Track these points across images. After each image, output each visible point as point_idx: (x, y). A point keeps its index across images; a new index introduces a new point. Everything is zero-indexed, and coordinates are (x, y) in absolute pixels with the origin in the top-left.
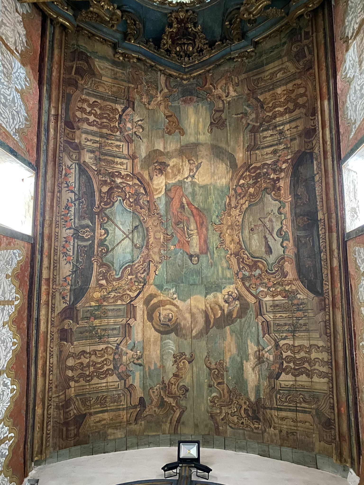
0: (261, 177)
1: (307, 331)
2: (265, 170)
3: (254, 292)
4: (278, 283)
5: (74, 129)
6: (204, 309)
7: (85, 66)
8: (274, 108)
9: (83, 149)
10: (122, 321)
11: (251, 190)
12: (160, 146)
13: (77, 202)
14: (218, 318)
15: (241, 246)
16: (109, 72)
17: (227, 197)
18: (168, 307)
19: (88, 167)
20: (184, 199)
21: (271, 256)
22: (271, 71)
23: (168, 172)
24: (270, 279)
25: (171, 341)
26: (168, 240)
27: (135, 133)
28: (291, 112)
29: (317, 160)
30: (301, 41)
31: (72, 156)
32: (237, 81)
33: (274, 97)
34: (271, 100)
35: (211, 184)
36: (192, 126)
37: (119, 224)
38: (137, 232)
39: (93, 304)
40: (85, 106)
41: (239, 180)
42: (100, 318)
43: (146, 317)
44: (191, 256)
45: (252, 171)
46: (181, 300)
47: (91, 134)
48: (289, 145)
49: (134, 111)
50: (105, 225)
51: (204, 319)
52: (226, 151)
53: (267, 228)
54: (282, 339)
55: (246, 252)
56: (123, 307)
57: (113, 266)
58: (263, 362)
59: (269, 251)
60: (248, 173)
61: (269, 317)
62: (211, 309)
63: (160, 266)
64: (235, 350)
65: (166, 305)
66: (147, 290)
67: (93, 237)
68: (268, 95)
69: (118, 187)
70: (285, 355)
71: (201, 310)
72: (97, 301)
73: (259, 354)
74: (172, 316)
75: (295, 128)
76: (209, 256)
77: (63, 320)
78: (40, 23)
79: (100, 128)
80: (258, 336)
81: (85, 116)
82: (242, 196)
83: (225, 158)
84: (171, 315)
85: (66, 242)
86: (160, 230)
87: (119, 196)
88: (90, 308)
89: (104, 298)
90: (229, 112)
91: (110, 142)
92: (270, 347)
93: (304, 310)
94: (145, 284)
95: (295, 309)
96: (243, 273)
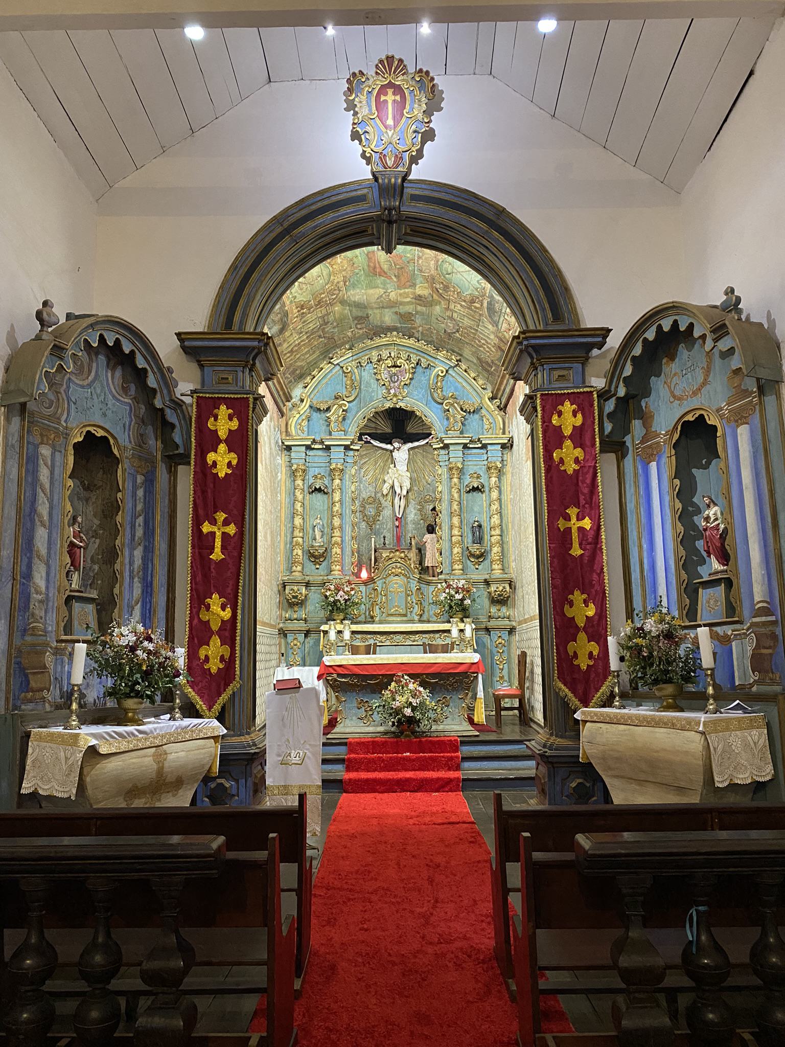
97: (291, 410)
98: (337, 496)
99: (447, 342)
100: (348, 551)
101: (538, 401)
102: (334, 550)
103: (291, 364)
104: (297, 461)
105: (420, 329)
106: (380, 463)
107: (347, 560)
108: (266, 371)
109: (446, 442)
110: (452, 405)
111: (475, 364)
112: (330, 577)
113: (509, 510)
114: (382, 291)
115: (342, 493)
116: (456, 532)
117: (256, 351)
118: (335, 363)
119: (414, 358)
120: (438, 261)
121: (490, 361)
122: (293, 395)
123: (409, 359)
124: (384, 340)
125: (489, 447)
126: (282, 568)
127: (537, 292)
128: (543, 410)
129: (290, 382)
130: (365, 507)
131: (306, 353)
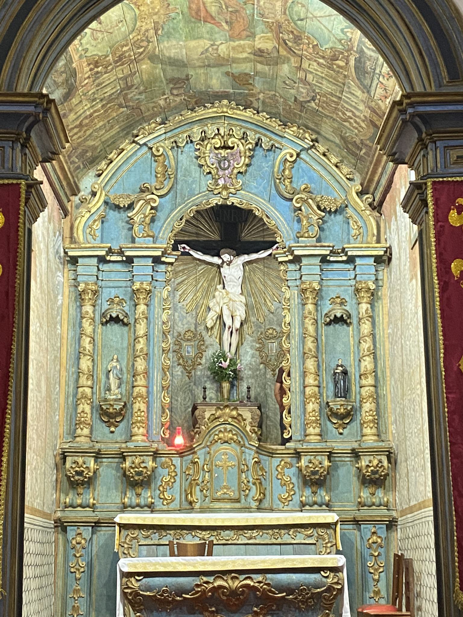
7: (350, 146)
13: (377, 71)
16: (323, 129)
19: (358, 87)
27: (295, 83)
28: (86, 118)
32: (155, 109)
37: (325, 31)
38: (299, 16)
40: (355, 125)
41: (144, 51)
49: (296, 98)
68: (115, 114)
78: (383, 208)
81: (358, 120)
91: (330, 90)
97: (77, 207)
98: (141, 329)
99: (296, 114)
100: (156, 407)
101: (429, 191)
102: (136, 406)
103: (79, 144)
104: (84, 278)
105: (261, 96)
106: (203, 283)
107: (155, 419)
108: (43, 147)
109: (296, 253)
110: (305, 201)
111: (337, 145)
112: (131, 445)
113: (385, 348)
114: (208, 43)
115: (148, 324)
116: (310, 380)
117: (31, 119)
118: (141, 143)
119: (252, 137)
121: (358, 142)
122: (82, 186)
123: (244, 137)
124: (210, 111)
125: (358, 261)
126: (61, 431)
127: (426, 40)
128: (436, 204)
129: (78, 168)
130: (181, 346)
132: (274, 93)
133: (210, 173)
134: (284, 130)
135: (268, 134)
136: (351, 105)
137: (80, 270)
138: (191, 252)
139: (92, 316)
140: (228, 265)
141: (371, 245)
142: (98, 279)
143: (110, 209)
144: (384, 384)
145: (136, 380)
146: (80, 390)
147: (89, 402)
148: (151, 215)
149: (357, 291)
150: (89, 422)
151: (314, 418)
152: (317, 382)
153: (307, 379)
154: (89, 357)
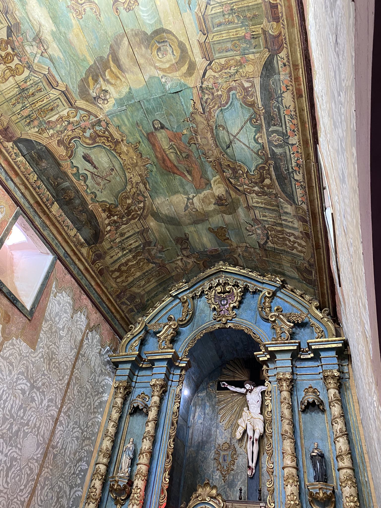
0: (125, 214)
1: (8, 99)
2: (124, 220)
3: (82, 112)
4: (62, 132)
5: (305, 233)
6: (126, 74)
7: (305, 274)
8: (137, 262)
9: (294, 216)
10: (213, 37)
11: (129, 201)
12: (228, 218)
14: (107, 69)
15: (116, 152)
16: (285, 269)
17: (149, 189)
18: (167, 65)
19: (287, 201)
20: (190, 178)
21: (83, 154)
22: (151, 283)
23: (213, 199)
24: (73, 132)
25: (148, 22)
26: (192, 138)
27: (252, 226)
29: (82, 245)
30: (135, 306)
31: (302, 212)
33: (141, 269)
34: (142, 266)
35: (169, 197)
36: (203, 235)
38: (226, 142)
39: (251, 56)
40: (300, 248)
41: (144, 206)
42: (239, 39)
43: (188, 47)
44: (163, 127)
45: (136, 216)
46: (155, 77)
47: (289, 226)
48: (112, 243)
50: (260, 147)
51: (121, 63)
52: (166, 223)
53: (99, 176)
54: (28, 77)
55: (108, 148)
56: (217, 55)
57: (241, 104)
58: (34, 39)
59: (86, 158)
60: (139, 212)
61: (54, 94)
62: (119, 78)
63: (191, 110)
64: (71, 39)
65: (170, 67)
66: (196, 80)
67: (269, 135)
68: (147, 269)
69: (256, 183)
70: (16, 61)
71: (129, 72)
72: (247, 60)
73: (43, 46)
74: (158, 55)
75: (112, 257)
76: (144, 132)
77: (280, 34)
79: (283, 230)
80: (55, 67)
81: (298, 241)
82: (136, 194)
83: (165, 218)
84: (160, 56)
85: (294, 131)
86: (204, 147)
87: (253, 175)
88: (254, 50)
89: (240, 64)
90: (176, 249)
91: (273, 220)
92: (36, 61)
93: (23, 119)
94: (201, 87)
95: (33, 115)
96: (101, 128)
98: (152, 414)
106: (236, 408)
109: (270, 349)
111: (299, 282)
113: (359, 434)
120: (212, 129)
124: (213, 270)
125: (323, 354)
129: (131, 310)
130: (219, 454)
131: (139, 279)
132: (245, 244)
133: (214, 309)
134: (262, 278)
135: (253, 282)
136: (291, 228)
137: (118, 372)
138: (228, 387)
139: (120, 406)
140: (250, 392)
141: (330, 339)
142: (132, 381)
143: (151, 336)
144: (364, 470)
145: (140, 458)
146: (97, 466)
147: (100, 477)
148: (172, 335)
149: (325, 378)
150: (97, 497)
151: (292, 503)
152: (294, 464)
153: (285, 459)
154: (109, 438)
